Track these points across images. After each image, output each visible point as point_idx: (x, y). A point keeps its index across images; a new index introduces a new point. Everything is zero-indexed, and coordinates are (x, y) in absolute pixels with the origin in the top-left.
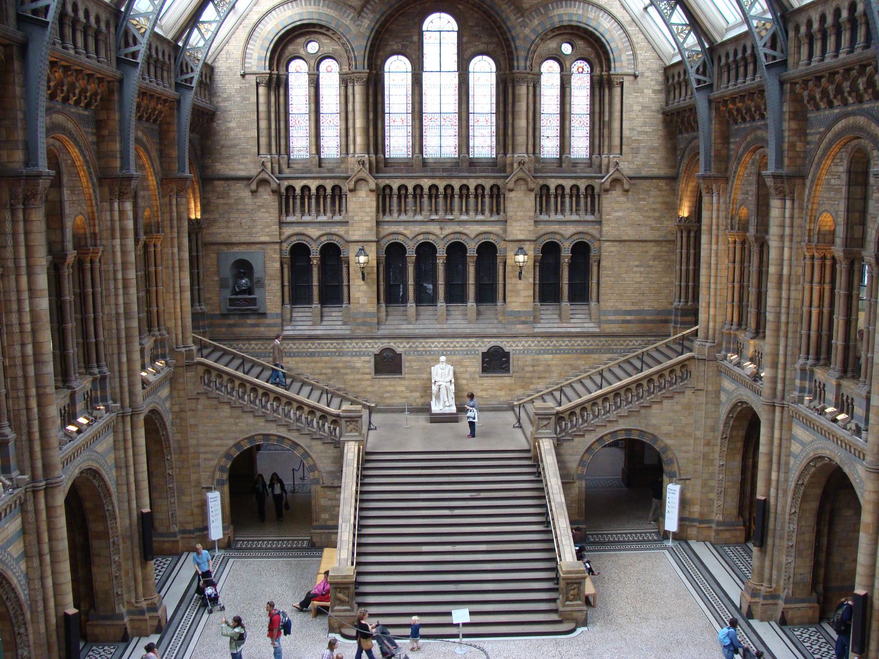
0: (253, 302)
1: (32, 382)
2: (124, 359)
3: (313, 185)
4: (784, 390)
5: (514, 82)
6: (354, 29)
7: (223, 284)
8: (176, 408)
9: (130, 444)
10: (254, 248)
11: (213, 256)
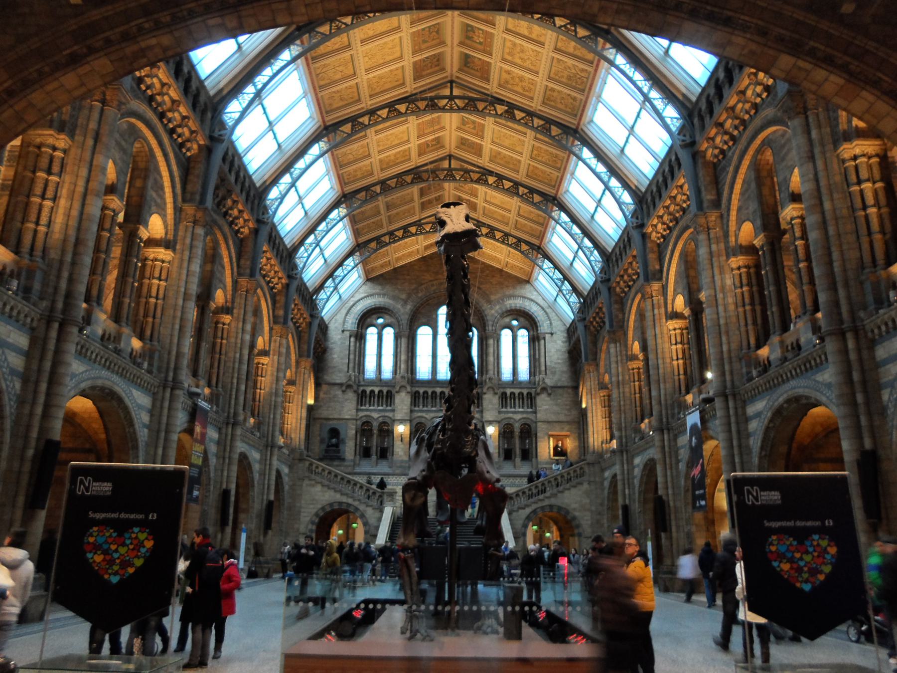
0: (339, 452)
1: (236, 370)
2: (272, 416)
3: (376, 390)
4: (626, 443)
5: (487, 338)
6: (402, 310)
7: (322, 441)
8: (291, 483)
9: (268, 462)
10: (341, 422)
11: (318, 426)
